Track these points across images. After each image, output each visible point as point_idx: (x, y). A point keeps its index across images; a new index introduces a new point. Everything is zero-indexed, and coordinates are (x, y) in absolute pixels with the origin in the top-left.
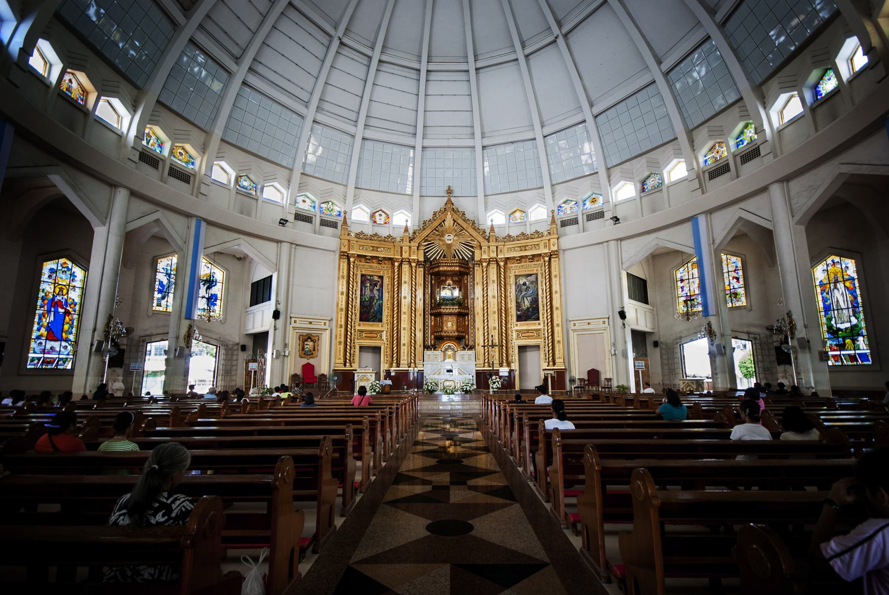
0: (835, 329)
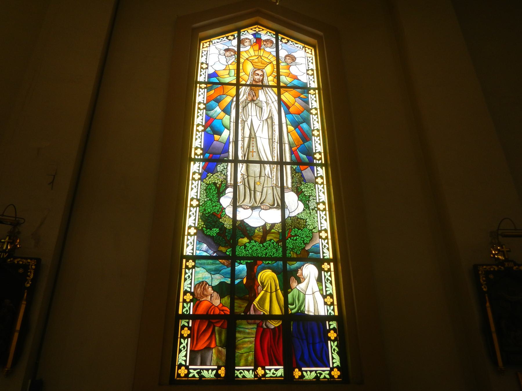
0: (228, 225)
